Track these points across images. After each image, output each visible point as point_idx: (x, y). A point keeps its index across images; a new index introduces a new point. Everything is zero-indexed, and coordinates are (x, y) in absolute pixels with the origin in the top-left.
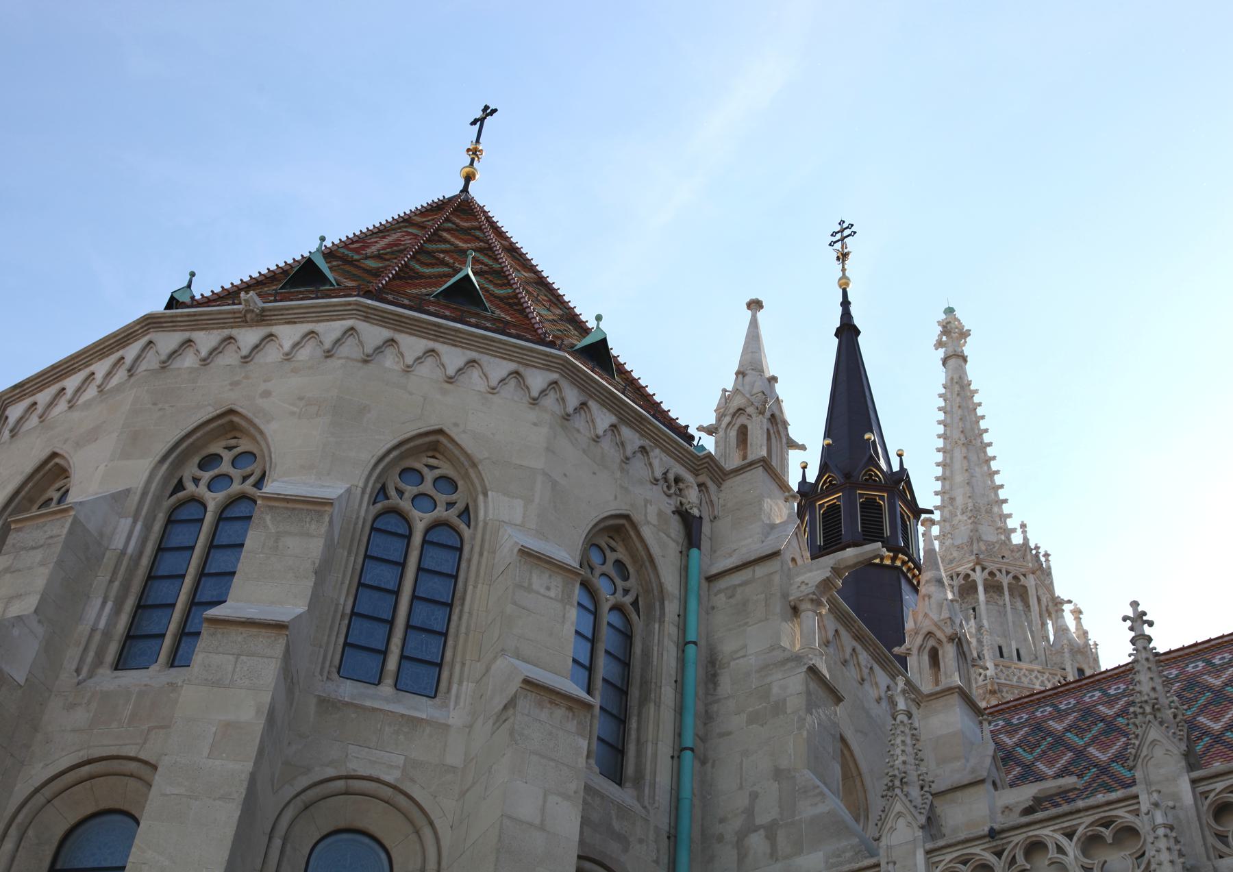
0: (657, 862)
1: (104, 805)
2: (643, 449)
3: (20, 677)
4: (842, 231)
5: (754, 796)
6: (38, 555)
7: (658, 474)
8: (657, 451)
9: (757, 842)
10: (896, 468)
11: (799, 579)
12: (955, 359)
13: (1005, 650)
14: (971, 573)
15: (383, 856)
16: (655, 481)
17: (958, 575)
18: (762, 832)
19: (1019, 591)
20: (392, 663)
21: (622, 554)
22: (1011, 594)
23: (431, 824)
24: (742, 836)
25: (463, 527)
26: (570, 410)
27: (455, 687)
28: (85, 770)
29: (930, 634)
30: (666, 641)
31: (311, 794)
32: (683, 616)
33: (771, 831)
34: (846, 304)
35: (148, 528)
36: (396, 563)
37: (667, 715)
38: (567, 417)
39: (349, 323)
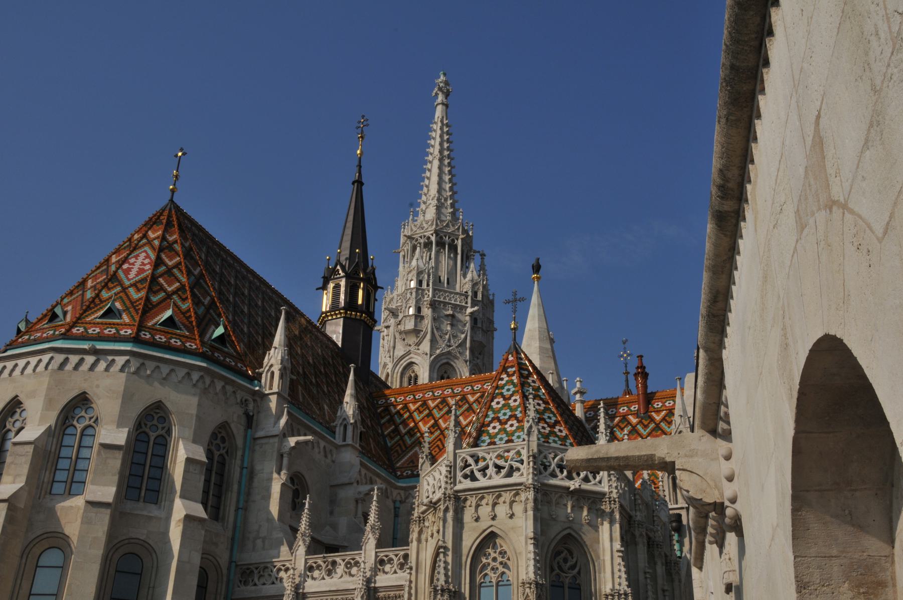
1: (51, 546)
2: (234, 392)
3: (22, 506)
5: (260, 526)
7: (239, 400)
8: (239, 391)
9: (259, 542)
14: (431, 236)
15: (140, 560)
16: (238, 403)
17: (425, 236)
18: (261, 540)
22: (450, 249)
23: (155, 552)
25: (167, 437)
26: (207, 386)
27: (163, 503)
28: (45, 536)
31: (118, 545)
32: (243, 456)
33: (264, 539)
36: (144, 453)
37: (234, 495)
38: (206, 389)
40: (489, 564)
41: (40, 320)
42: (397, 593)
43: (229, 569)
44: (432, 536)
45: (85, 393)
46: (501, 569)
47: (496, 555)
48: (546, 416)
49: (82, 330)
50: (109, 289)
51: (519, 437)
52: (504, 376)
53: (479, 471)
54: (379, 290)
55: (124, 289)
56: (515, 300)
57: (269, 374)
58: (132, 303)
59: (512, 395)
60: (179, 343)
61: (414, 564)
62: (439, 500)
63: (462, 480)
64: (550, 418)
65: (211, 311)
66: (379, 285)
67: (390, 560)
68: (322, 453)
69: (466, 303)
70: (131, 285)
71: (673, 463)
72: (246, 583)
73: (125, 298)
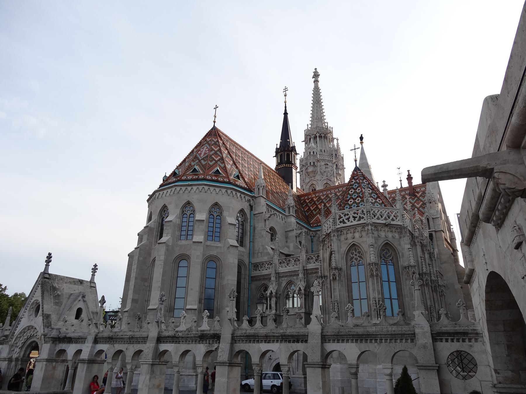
0: (247, 257)
3: (171, 245)
4: (285, 91)
5: (259, 248)
7: (247, 200)
8: (246, 196)
9: (259, 254)
10: (293, 146)
11: (266, 216)
12: (316, 82)
13: (322, 150)
18: (260, 253)
19: (325, 137)
20: (214, 238)
24: (258, 253)
29: (289, 205)
30: (248, 226)
31: (206, 258)
32: (250, 222)
33: (261, 253)
34: (286, 107)
35: (181, 219)
37: (248, 237)
38: (233, 196)
40: (353, 257)
41: (170, 176)
42: (316, 271)
43: (249, 265)
44: (328, 247)
45: (189, 201)
46: (359, 259)
47: (357, 253)
49: (185, 177)
50: (194, 161)
51: (362, 204)
53: (346, 219)
55: (200, 161)
56: (355, 149)
57: (257, 189)
58: (203, 166)
61: (322, 259)
62: (330, 232)
63: (340, 224)
64: (374, 196)
66: (297, 153)
67: (312, 258)
68: (281, 219)
69: (332, 159)
71: (493, 169)
72: (256, 270)
73: (200, 164)
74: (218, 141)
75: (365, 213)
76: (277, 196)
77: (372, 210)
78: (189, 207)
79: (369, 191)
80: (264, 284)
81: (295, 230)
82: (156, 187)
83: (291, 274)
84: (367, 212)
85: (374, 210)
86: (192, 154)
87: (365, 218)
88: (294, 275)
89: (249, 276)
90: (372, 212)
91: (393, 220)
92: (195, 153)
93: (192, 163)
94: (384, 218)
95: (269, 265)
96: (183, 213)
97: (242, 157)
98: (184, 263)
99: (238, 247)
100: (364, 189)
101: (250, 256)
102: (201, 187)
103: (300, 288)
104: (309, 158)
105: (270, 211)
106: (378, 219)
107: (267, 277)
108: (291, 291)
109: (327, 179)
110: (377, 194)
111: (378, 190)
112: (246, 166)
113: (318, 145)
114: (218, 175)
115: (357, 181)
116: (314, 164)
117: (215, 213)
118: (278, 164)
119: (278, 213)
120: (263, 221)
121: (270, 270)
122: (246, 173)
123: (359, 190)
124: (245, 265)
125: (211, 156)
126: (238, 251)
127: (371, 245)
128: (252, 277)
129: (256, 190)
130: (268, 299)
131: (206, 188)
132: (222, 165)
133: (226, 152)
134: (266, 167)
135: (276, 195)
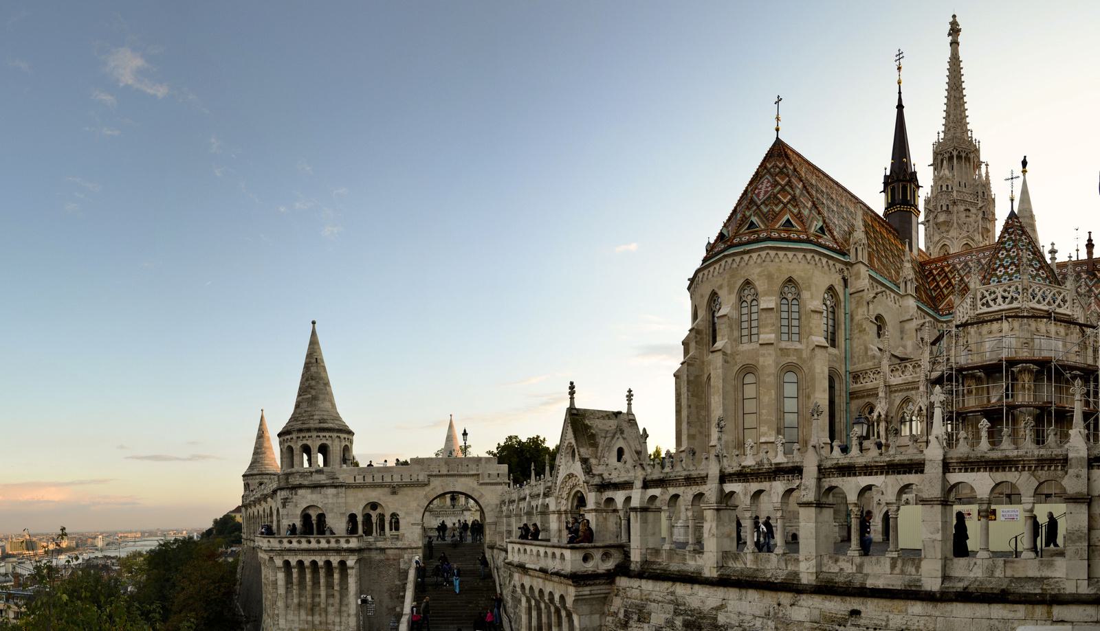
6: (724, 326)
21: (831, 293)
32: (845, 306)
37: (843, 331)
38: (816, 264)
39: (767, 251)
43: (846, 376)
48: (1033, 263)
51: (1016, 277)
52: (1006, 235)
54: (921, 188)
55: (758, 207)
57: (854, 250)
58: (764, 215)
59: (1012, 248)
60: (796, 236)
64: (1036, 264)
65: (813, 212)
70: (762, 204)
72: (856, 383)
73: (759, 213)
74: (785, 166)
75: (1020, 291)
76: (887, 262)
77: (1031, 287)
78: (749, 289)
79: (1029, 255)
80: (869, 403)
81: (915, 320)
82: (698, 264)
83: (908, 387)
84: (1023, 290)
85: (1034, 287)
86: (745, 196)
87: (1020, 299)
88: (912, 389)
89: (846, 392)
90: (1030, 291)
91: (1059, 306)
92: (750, 195)
93: (746, 212)
94: (1047, 301)
95: (875, 375)
96: (741, 300)
97: (828, 194)
98: (750, 379)
99: (827, 347)
100: (1022, 251)
101: (847, 362)
102: (763, 254)
103: (921, 408)
104: (940, 197)
105: (875, 288)
106: (1039, 302)
107: (873, 393)
108: (908, 412)
109: (968, 237)
110: (1040, 262)
111: (1043, 257)
112: (835, 209)
113: (955, 174)
114: (789, 228)
115: (1013, 236)
116: (948, 209)
117: (790, 295)
118: (889, 206)
119: (888, 292)
120: (865, 303)
121: (878, 382)
122: (834, 223)
123: (1014, 252)
124: (839, 376)
125: (775, 196)
126: (827, 355)
127: (1025, 343)
128: (851, 394)
129: (853, 251)
130: (875, 424)
131: (772, 253)
132: (796, 211)
133: (800, 185)
134: (868, 210)
135: (884, 260)
